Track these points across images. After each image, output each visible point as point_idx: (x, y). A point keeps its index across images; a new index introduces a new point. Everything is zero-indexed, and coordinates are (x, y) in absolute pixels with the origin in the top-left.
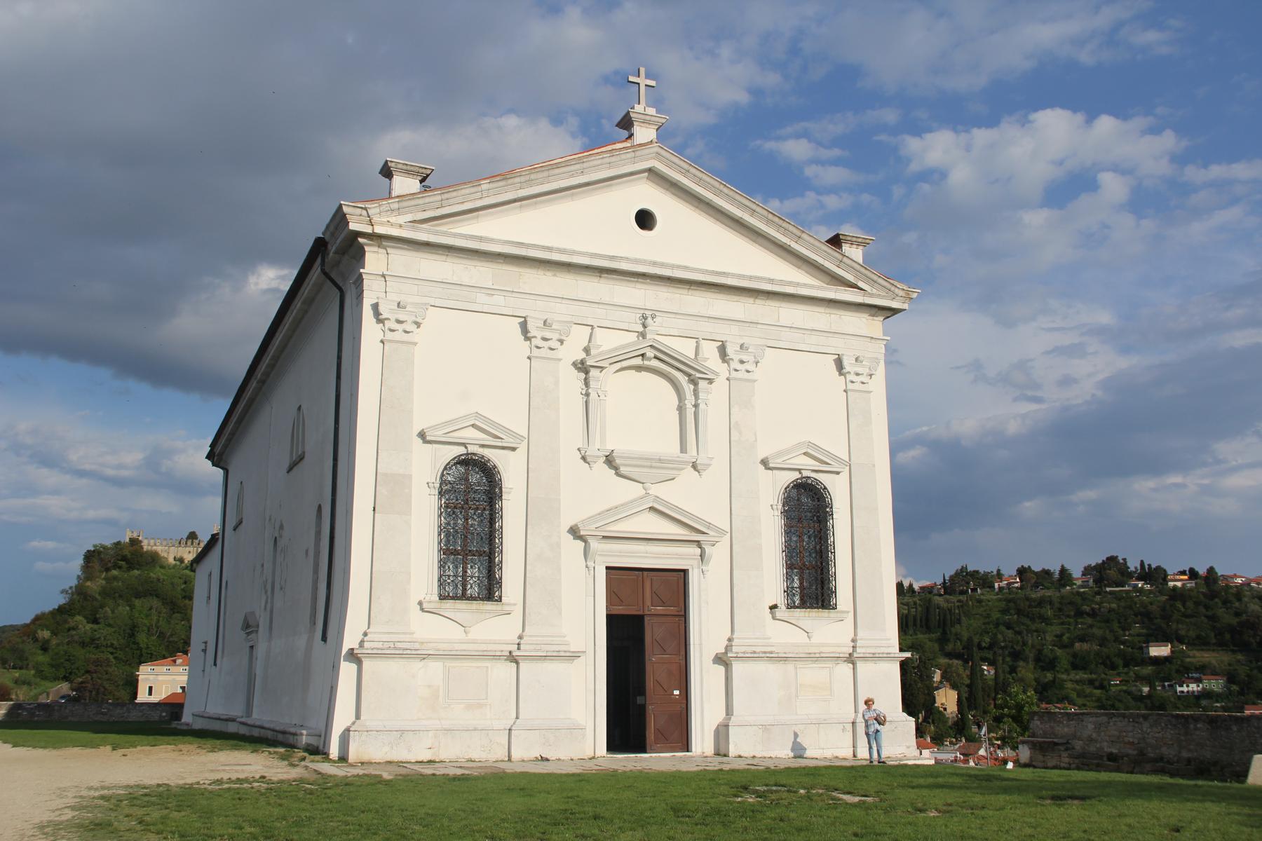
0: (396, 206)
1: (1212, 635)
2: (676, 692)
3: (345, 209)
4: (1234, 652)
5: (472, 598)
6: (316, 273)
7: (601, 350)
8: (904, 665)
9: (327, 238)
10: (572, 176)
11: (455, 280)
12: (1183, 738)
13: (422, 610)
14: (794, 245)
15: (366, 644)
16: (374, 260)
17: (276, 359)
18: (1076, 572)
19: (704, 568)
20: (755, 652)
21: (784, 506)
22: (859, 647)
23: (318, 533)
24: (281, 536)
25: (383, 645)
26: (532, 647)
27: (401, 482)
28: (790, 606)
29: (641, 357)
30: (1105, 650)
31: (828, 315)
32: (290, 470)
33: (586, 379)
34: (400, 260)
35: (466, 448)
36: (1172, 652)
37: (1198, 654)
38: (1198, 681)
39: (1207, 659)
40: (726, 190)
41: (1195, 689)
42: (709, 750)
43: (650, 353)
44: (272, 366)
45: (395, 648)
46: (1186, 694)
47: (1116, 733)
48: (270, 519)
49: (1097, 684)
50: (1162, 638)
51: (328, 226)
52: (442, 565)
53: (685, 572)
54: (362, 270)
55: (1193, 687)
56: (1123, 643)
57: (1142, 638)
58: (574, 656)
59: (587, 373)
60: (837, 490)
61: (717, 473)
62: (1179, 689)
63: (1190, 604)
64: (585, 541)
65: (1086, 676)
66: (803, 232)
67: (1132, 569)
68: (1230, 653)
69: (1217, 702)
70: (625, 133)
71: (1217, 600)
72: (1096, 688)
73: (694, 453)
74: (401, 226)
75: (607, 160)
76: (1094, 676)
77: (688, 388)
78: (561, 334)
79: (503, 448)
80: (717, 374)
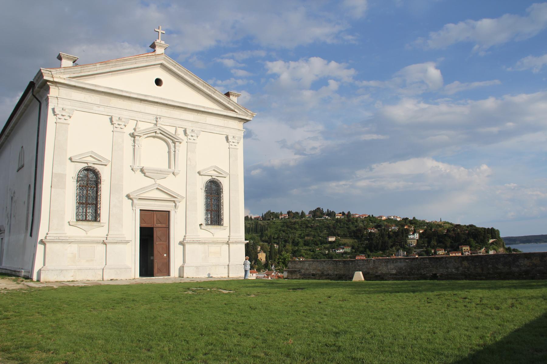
0: (63, 71)
1: (348, 234)
2: (165, 255)
3: (42, 71)
4: (354, 239)
5: (89, 221)
6: (30, 95)
7: (140, 129)
8: (247, 246)
9: (35, 82)
10: (132, 64)
11: (85, 101)
12: (335, 268)
13: (70, 225)
14: (213, 95)
15: (48, 238)
16: (53, 92)
17: (13, 128)
18: (307, 213)
19: (176, 210)
20: (194, 241)
21: (205, 188)
22: (231, 239)
23: (29, 195)
24: (14, 196)
25: (54, 238)
29: (155, 133)
30: (315, 239)
32: (18, 171)
33: (134, 140)
34: (64, 92)
35: (88, 164)
36: (335, 239)
37: (343, 240)
38: (343, 248)
39: (346, 242)
40: (189, 73)
41: (342, 251)
42: (177, 275)
43: (158, 131)
44: (11, 130)
45: (59, 239)
47: (315, 267)
48: (10, 190)
49: (312, 250)
50: (333, 235)
51: (35, 77)
52: (78, 208)
53: (169, 212)
54: (48, 95)
55: (341, 251)
56: (321, 237)
57: (327, 235)
58: (127, 242)
59: (134, 138)
60: (225, 184)
62: (337, 251)
63: (342, 224)
64: (132, 200)
65: (308, 248)
66: (216, 90)
67: (325, 212)
68: (353, 239)
69: (348, 255)
70: (153, 50)
71: (350, 222)
72: (311, 252)
73: (174, 169)
74: (64, 79)
75: (146, 59)
76: (311, 248)
77: (172, 145)
78: (125, 123)
79: (102, 165)
80: (183, 140)
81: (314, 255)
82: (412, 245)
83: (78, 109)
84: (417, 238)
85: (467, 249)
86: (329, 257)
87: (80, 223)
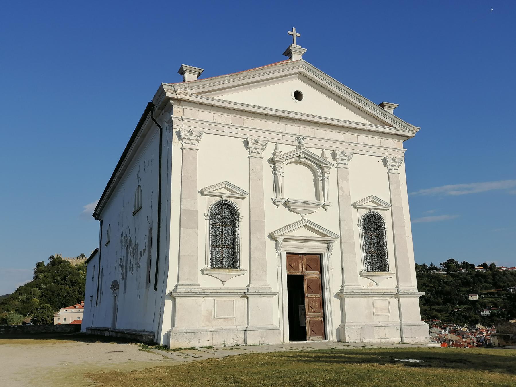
0: (187, 85)
3: (164, 86)
7: (280, 154)
8: (421, 298)
11: (215, 121)
13: (203, 273)
15: (178, 291)
16: (177, 111)
17: (126, 166)
20: (354, 292)
21: (363, 225)
22: (400, 290)
25: (185, 290)
26: (254, 291)
27: (193, 213)
28: (368, 271)
29: (298, 157)
31: (379, 139)
33: (274, 167)
34: (189, 112)
35: (222, 198)
40: (334, 82)
42: (335, 339)
43: (303, 156)
44: (124, 170)
51: (155, 96)
53: (320, 255)
54: (172, 116)
59: (275, 164)
60: (386, 217)
61: (333, 210)
64: (276, 241)
66: (369, 101)
70: (288, 57)
77: (319, 172)
78: (263, 146)
79: (239, 198)
80: (332, 165)
83: (207, 131)
87: (216, 270)
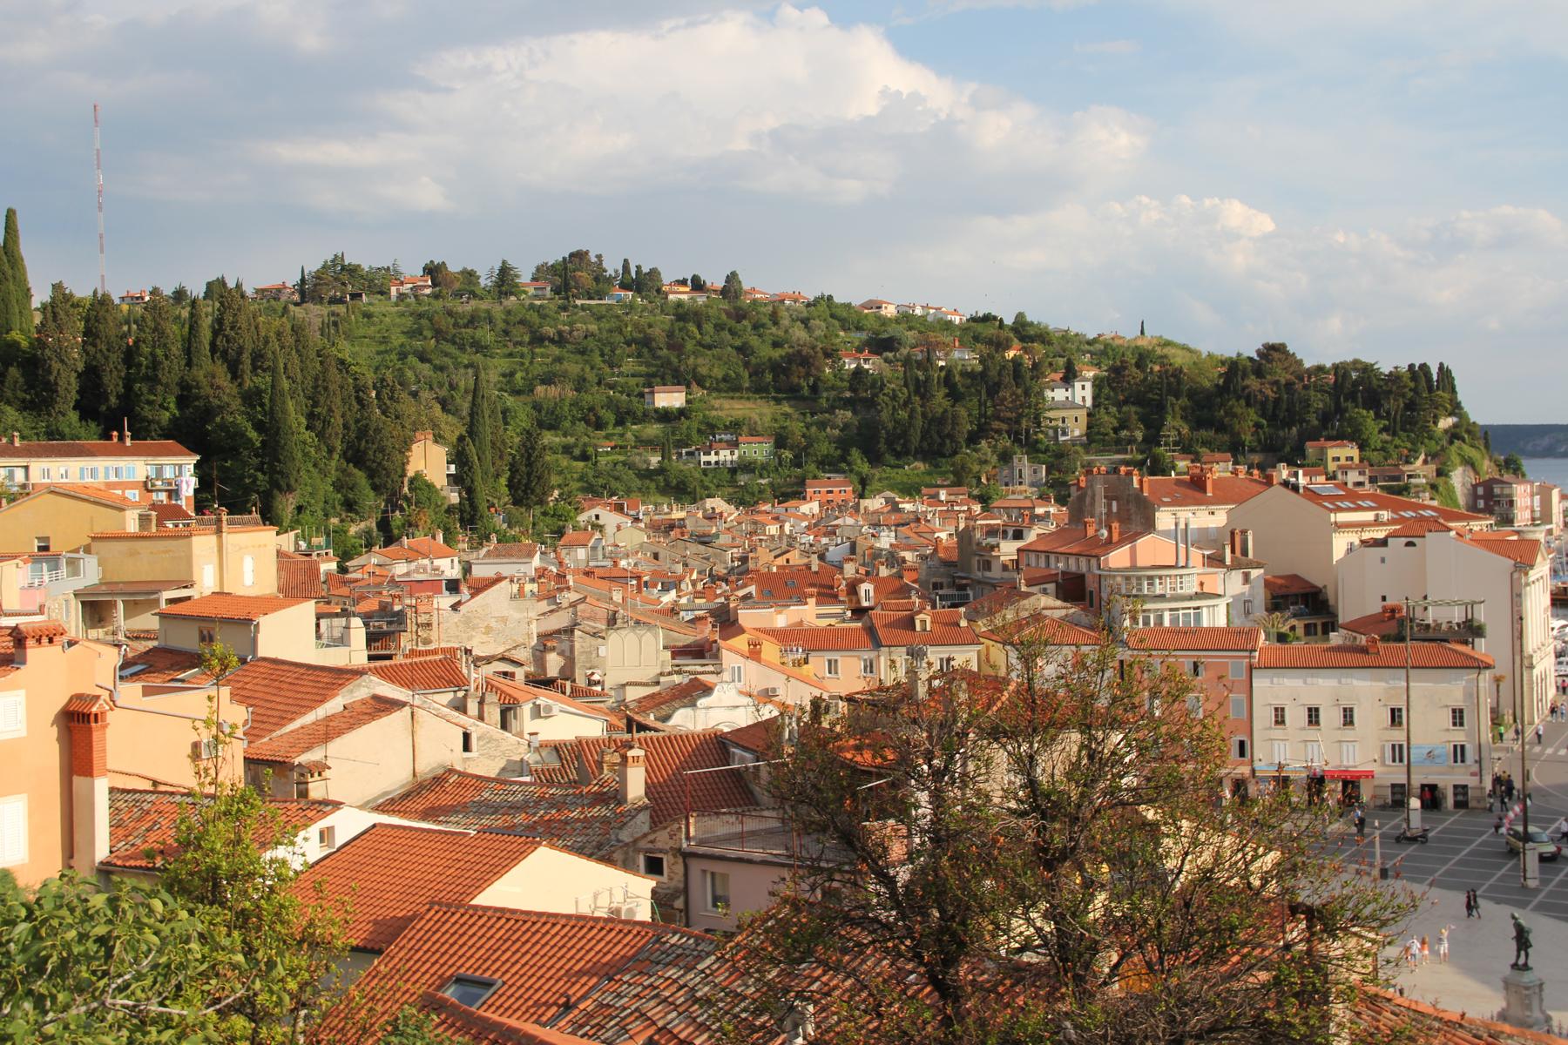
1: (746, 374)
4: (778, 401)
30: (588, 398)
36: (688, 402)
37: (726, 404)
38: (734, 445)
39: (740, 412)
41: (729, 458)
46: (713, 466)
49: (577, 452)
50: (677, 378)
55: (725, 455)
56: (611, 387)
57: (641, 380)
62: (704, 458)
63: (708, 327)
65: (557, 440)
67: (610, 272)
68: (772, 403)
69: (761, 476)
71: (745, 322)
72: (576, 459)
76: (571, 440)
81: (591, 473)
82: (1064, 434)
84: (1089, 403)
85: (1351, 459)
86: (667, 484)
